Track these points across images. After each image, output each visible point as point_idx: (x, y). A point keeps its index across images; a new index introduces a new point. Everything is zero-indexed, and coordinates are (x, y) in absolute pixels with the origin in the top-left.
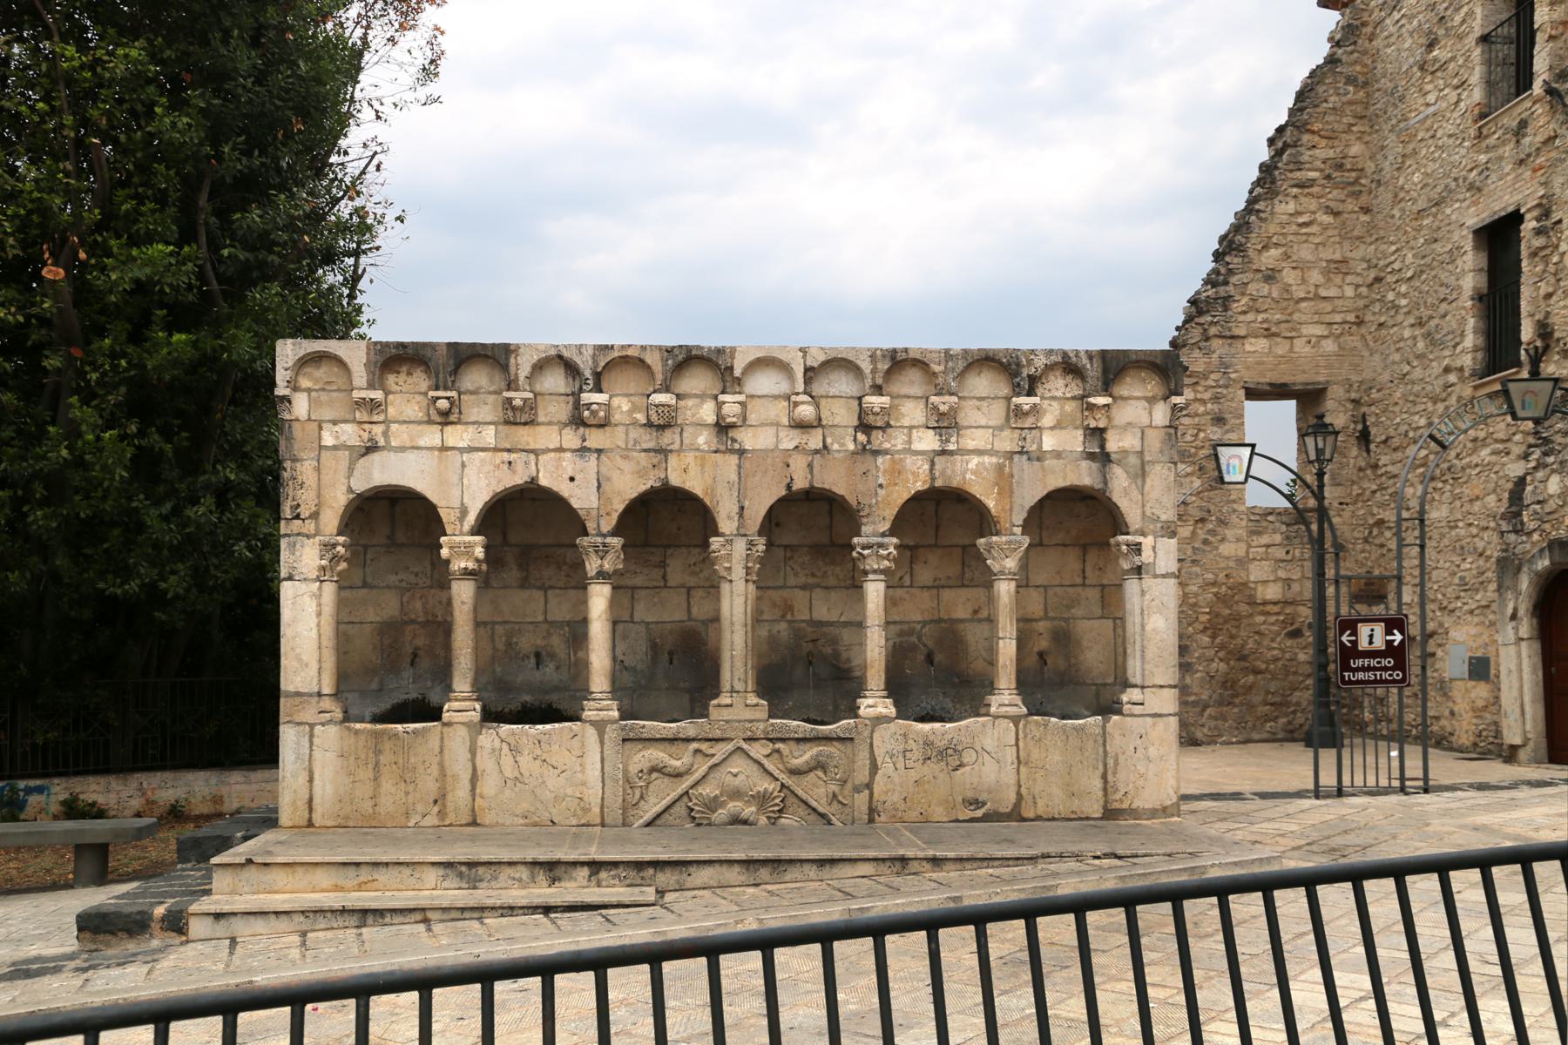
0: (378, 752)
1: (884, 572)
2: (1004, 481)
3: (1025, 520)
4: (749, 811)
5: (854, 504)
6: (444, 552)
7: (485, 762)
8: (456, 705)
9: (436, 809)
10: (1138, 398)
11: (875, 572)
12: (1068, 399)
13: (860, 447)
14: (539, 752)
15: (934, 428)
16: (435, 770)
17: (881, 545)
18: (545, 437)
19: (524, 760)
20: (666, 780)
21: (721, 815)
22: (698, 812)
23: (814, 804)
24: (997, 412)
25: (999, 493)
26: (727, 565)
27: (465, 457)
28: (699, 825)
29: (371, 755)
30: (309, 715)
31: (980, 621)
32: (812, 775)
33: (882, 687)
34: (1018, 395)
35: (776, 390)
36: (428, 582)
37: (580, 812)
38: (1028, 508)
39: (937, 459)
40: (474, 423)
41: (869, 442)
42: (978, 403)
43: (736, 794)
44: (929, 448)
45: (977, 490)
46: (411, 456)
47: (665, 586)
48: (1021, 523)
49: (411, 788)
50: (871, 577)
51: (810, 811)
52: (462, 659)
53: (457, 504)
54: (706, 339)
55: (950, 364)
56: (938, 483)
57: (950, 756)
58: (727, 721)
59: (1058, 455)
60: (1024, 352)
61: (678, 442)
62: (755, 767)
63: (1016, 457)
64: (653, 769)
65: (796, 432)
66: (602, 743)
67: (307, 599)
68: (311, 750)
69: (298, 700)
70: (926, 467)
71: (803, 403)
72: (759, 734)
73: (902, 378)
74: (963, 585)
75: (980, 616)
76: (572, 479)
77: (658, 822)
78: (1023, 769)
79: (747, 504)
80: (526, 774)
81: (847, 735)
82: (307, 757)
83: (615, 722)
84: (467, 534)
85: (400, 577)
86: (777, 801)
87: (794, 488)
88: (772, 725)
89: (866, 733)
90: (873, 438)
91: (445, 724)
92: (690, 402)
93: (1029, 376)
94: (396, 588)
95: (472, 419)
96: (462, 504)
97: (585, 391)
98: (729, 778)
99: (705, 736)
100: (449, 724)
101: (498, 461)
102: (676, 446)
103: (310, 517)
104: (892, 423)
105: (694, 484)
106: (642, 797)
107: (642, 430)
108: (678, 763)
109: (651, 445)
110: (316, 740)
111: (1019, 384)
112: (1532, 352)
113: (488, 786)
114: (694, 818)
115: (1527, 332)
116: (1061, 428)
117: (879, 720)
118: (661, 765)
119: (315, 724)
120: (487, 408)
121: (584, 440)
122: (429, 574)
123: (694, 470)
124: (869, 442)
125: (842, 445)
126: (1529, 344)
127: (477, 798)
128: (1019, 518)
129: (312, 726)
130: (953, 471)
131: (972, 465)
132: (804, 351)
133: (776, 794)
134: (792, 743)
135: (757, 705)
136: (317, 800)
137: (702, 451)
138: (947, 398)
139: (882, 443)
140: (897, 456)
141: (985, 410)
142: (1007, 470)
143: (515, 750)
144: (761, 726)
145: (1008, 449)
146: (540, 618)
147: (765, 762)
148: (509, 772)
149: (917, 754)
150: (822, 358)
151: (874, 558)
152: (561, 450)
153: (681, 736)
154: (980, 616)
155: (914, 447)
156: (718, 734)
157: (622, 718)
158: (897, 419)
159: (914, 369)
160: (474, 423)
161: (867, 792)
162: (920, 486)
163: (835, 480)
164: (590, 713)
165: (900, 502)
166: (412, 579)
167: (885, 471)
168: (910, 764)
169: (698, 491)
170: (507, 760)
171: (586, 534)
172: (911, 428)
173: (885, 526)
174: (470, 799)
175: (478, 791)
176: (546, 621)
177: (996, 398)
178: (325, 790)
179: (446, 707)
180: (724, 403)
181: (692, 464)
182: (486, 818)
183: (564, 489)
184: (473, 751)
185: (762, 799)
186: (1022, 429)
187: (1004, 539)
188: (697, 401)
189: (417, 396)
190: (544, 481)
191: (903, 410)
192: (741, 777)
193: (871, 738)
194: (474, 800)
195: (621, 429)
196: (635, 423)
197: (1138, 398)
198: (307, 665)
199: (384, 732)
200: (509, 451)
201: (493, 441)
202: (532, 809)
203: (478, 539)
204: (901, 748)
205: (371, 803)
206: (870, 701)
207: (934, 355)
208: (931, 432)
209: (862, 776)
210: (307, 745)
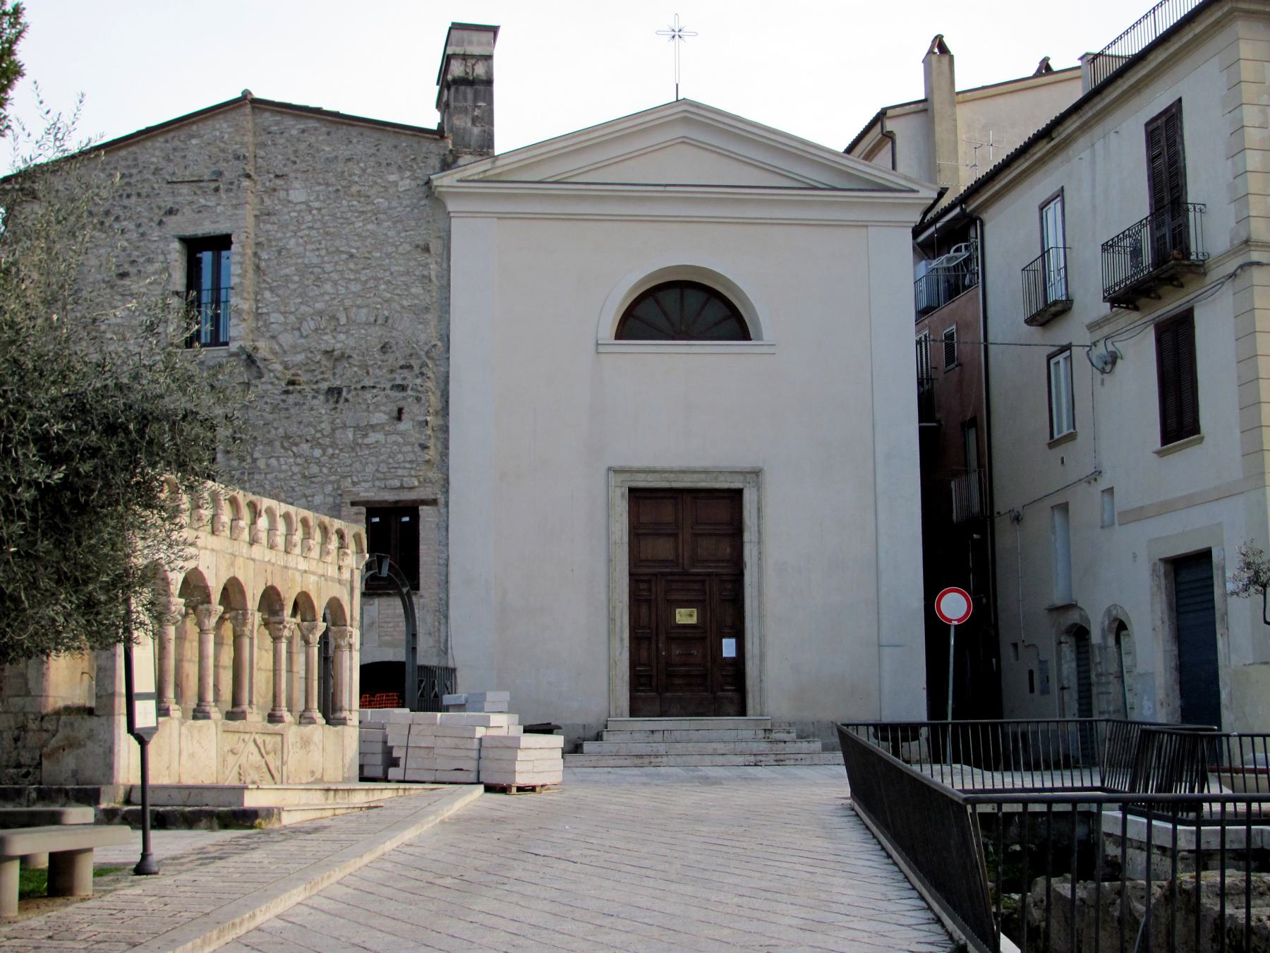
2: (319, 589)
100: (172, 719)
113: (184, 760)
149: (299, 745)
171: (209, 602)
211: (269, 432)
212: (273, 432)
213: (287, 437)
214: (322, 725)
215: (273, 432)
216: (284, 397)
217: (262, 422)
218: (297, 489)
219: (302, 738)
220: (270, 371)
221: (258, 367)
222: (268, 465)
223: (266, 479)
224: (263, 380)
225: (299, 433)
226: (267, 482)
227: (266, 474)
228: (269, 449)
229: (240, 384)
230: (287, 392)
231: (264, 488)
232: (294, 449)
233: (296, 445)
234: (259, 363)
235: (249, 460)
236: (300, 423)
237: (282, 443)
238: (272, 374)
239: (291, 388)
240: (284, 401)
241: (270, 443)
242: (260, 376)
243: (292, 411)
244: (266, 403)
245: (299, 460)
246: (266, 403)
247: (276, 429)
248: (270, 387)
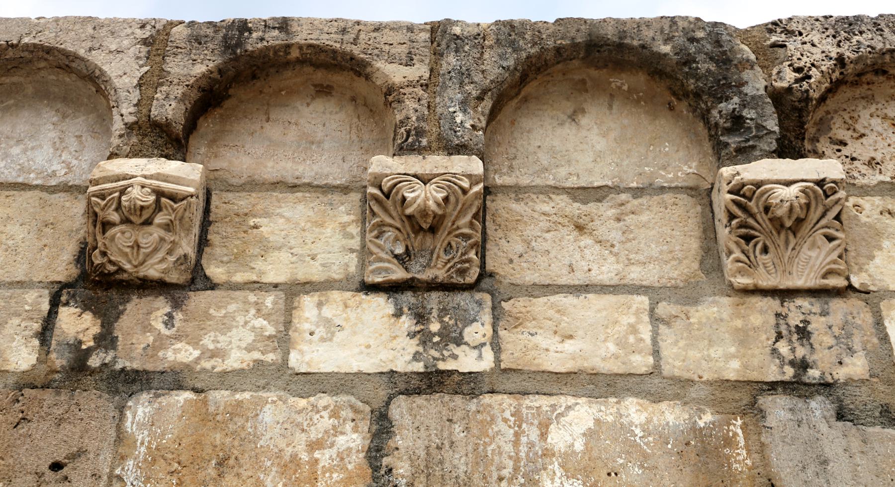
13: (59, 360)
15: (391, 288)
34: (744, 154)
39: (400, 409)
41: (106, 340)
42: (575, 208)
44: (368, 365)
55: (451, 60)
60: (745, 35)
73: (273, 131)
90: (124, 325)
93: (778, 97)
104: (215, 271)
111: (737, 122)
124: (106, 340)
130: (480, 458)
138: (436, 163)
139: (161, 342)
140: (220, 397)
141: (610, 231)
145: (733, 370)
155: (295, 361)
159: (319, 105)
167: (156, 456)
186: (785, 294)
191: (269, 228)
207: (388, 36)
208: (381, 305)
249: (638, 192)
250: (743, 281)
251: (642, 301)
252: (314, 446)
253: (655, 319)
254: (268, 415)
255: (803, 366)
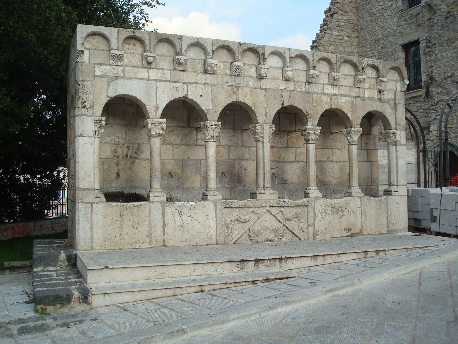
0: (121, 215)
1: (314, 140)
2: (353, 106)
3: (360, 123)
4: (272, 236)
5: (305, 113)
6: (150, 126)
7: (169, 219)
8: (156, 194)
9: (148, 240)
10: (392, 80)
11: (312, 140)
12: (372, 78)
14: (190, 214)
16: (147, 223)
17: (315, 130)
18: (189, 77)
19: (184, 217)
20: (240, 224)
21: (261, 238)
22: (253, 237)
23: (295, 232)
24: (350, 81)
25: (352, 112)
26: (262, 135)
27: (158, 84)
28: (253, 242)
29: (119, 217)
30: (90, 199)
31: (330, 161)
32: (293, 221)
33: (315, 186)
35: (277, 65)
36: (124, 141)
37: (208, 239)
38: (361, 118)
40: (162, 69)
43: (267, 229)
45: (345, 110)
46: (135, 82)
47: (220, 145)
48: (359, 123)
49: (137, 231)
50: (311, 142)
51: (293, 235)
52: (157, 173)
53: (154, 105)
54: (255, 41)
56: (333, 107)
57: (339, 211)
58: (263, 200)
59: (370, 99)
61: (242, 83)
62: (273, 218)
63: (357, 99)
64: (236, 220)
65: (285, 82)
66: (216, 209)
67: (89, 145)
68: (92, 215)
69: (85, 192)
70: (329, 100)
71: (289, 71)
72: (275, 205)
74: (324, 148)
75: (330, 160)
76: (201, 96)
77: (237, 242)
78: (363, 216)
79: (267, 111)
80: (186, 223)
81: (306, 205)
82: (90, 218)
83: (220, 200)
84: (159, 118)
85: (111, 138)
86: (282, 231)
87: (284, 105)
88: (280, 201)
89: (312, 204)
91: (150, 202)
92: (246, 67)
94: (110, 143)
95: (161, 67)
96: (156, 105)
97: (208, 58)
98: (264, 223)
99: (255, 206)
100: (153, 202)
101: (171, 87)
102: (242, 85)
103: (90, 108)
105: (248, 101)
106: (231, 232)
107: (229, 77)
108: (245, 218)
109: (232, 84)
110: (94, 210)
112: (426, 84)
113: (170, 229)
114: (251, 240)
115: (424, 77)
116: (370, 89)
117: (317, 198)
118: (239, 218)
119: (94, 203)
120: (167, 63)
121: (206, 80)
122: (124, 137)
123: (248, 95)
125: (301, 89)
126: (425, 82)
127: (165, 235)
128: (359, 121)
129: (92, 204)
130: (338, 102)
131: (343, 101)
132: (289, 50)
133: (281, 229)
134: (286, 208)
135: (274, 193)
136: (95, 238)
137: (251, 88)
140: (319, 95)
142: (354, 103)
143: (181, 214)
144: (276, 201)
145: (355, 95)
146: (171, 158)
147: (277, 215)
148: (179, 222)
149: (329, 212)
150: (296, 54)
151: (313, 134)
152: (197, 83)
153: (246, 206)
154: (330, 160)
155: (325, 92)
156: (260, 205)
157: (223, 199)
158: (319, 81)
160: (162, 69)
161: (313, 227)
162: (327, 107)
163: (298, 103)
164: (211, 197)
165: (321, 113)
166: (117, 139)
168: (327, 215)
169: (250, 104)
170: (177, 218)
172: (324, 84)
173: (316, 122)
174: (163, 235)
175: (166, 231)
176: (173, 159)
177: (350, 75)
178: (98, 234)
179: (151, 195)
180: (262, 68)
181: (248, 93)
182: (169, 244)
183: (198, 100)
184: (163, 214)
185: (276, 231)
187: (355, 129)
188: (249, 67)
189: (137, 55)
190: (190, 97)
192: (268, 222)
193: (314, 205)
194: (164, 235)
195: (220, 76)
196: (226, 74)
197: (392, 80)
198: (89, 176)
199: (124, 206)
200: (175, 82)
201: (169, 77)
202: (188, 239)
203: (164, 120)
204: (324, 209)
205: (119, 238)
206: (313, 191)
208: (331, 86)
209: (311, 221)
210: (90, 213)
211: (441, 39)
212: (443, 39)
213: (449, 40)
214: (360, 197)
215: (443, 39)
216: (446, 21)
217: (437, 36)
218: (455, 65)
219: (333, 207)
220: (439, 9)
221: (434, 9)
222: (442, 56)
223: (441, 63)
224: (436, 15)
225: (454, 36)
226: (442, 64)
227: (441, 60)
228: (442, 48)
229: (427, 20)
230: (447, 18)
231: (441, 68)
232: (453, 45)
233: (453, 43)
234: (434, 8)
235: (434, 56)
236: (454, 31)
237: (447, 43)
238: (440, 11)
239: (448, 15)
240: (446, 22)
241: (441, 45)
242: (435, 13)
243: (450, 26)
244: (439, 26)
245: (455, 50)
246: (439, 26)
247: (444, 37)
248: (439, 17)
249: (349, 76)
250: (356, 86)
251: (349, 88)
252: (326, 100)
253: (350, 90)
254: (323, 97)
255: (359, 95)
